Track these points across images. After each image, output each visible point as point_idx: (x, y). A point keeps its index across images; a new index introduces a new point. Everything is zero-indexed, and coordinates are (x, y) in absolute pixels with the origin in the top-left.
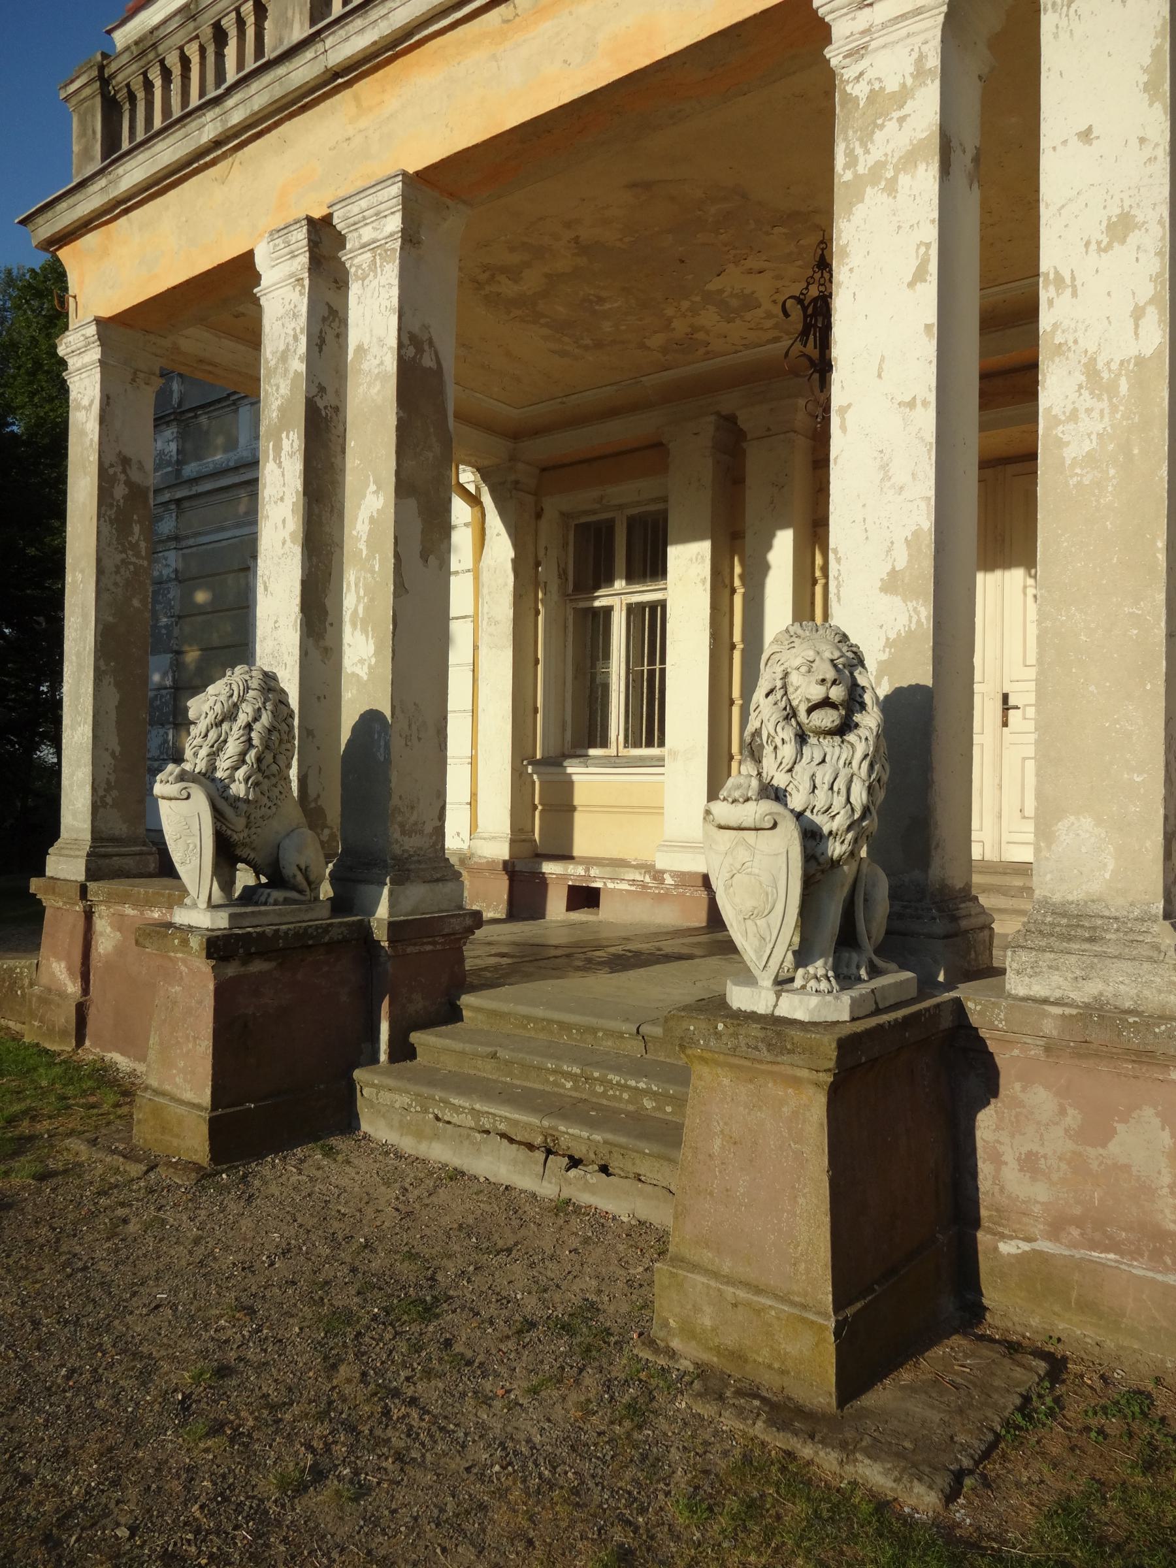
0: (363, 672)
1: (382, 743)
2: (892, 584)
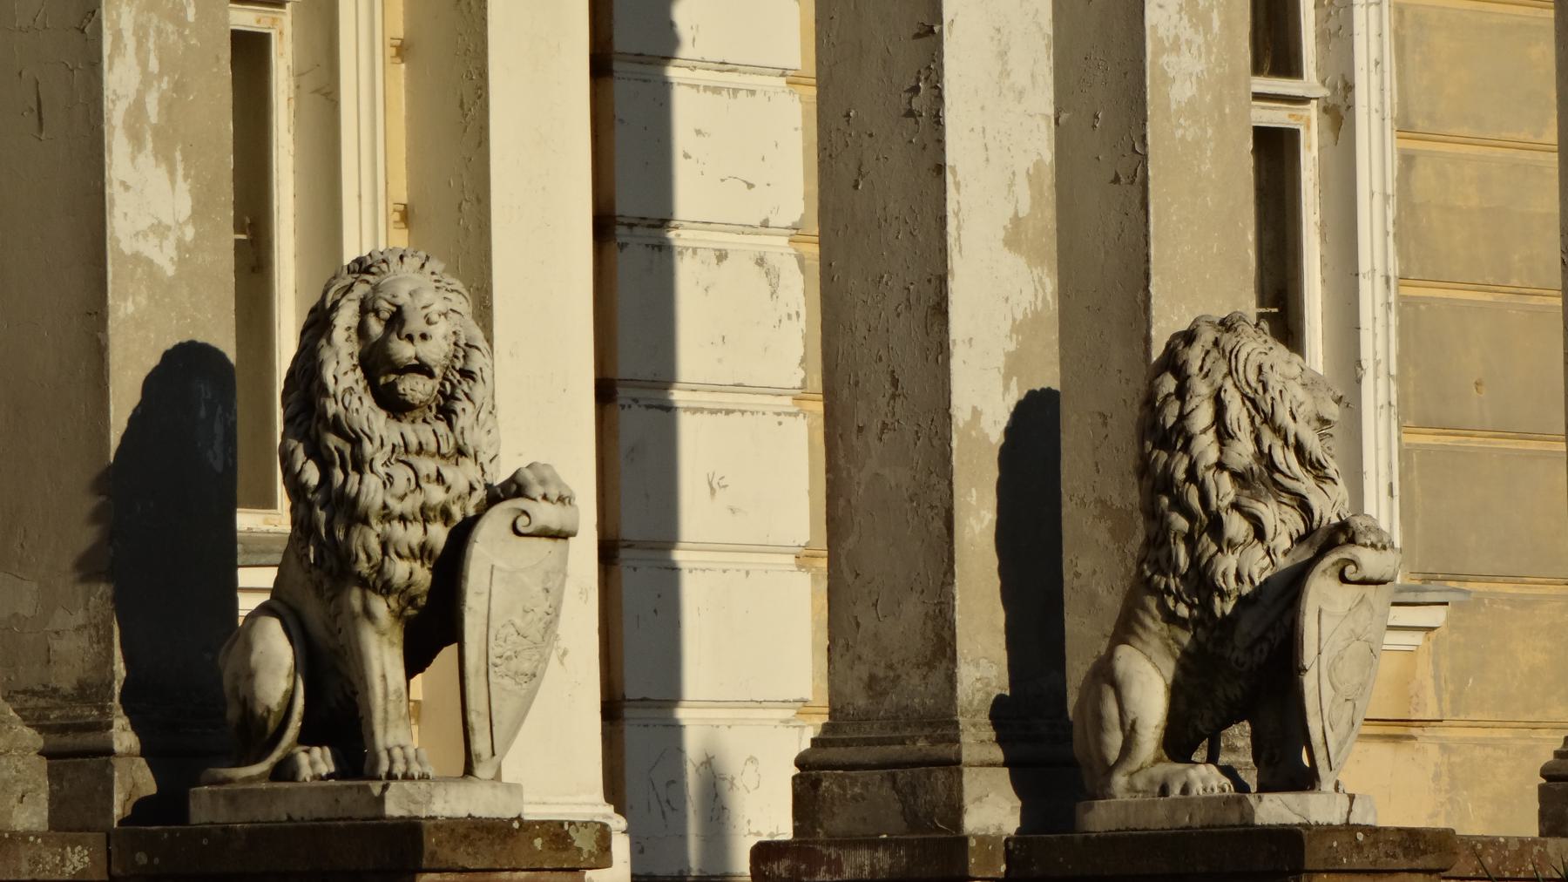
0: (164, 258)
1: (218, 429)
2: (1015, 238)
